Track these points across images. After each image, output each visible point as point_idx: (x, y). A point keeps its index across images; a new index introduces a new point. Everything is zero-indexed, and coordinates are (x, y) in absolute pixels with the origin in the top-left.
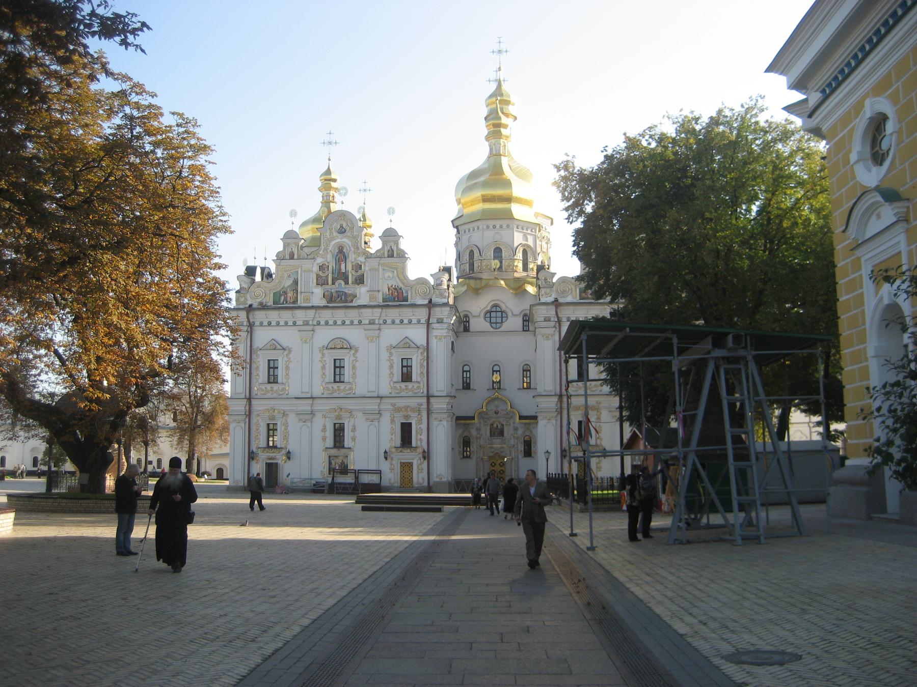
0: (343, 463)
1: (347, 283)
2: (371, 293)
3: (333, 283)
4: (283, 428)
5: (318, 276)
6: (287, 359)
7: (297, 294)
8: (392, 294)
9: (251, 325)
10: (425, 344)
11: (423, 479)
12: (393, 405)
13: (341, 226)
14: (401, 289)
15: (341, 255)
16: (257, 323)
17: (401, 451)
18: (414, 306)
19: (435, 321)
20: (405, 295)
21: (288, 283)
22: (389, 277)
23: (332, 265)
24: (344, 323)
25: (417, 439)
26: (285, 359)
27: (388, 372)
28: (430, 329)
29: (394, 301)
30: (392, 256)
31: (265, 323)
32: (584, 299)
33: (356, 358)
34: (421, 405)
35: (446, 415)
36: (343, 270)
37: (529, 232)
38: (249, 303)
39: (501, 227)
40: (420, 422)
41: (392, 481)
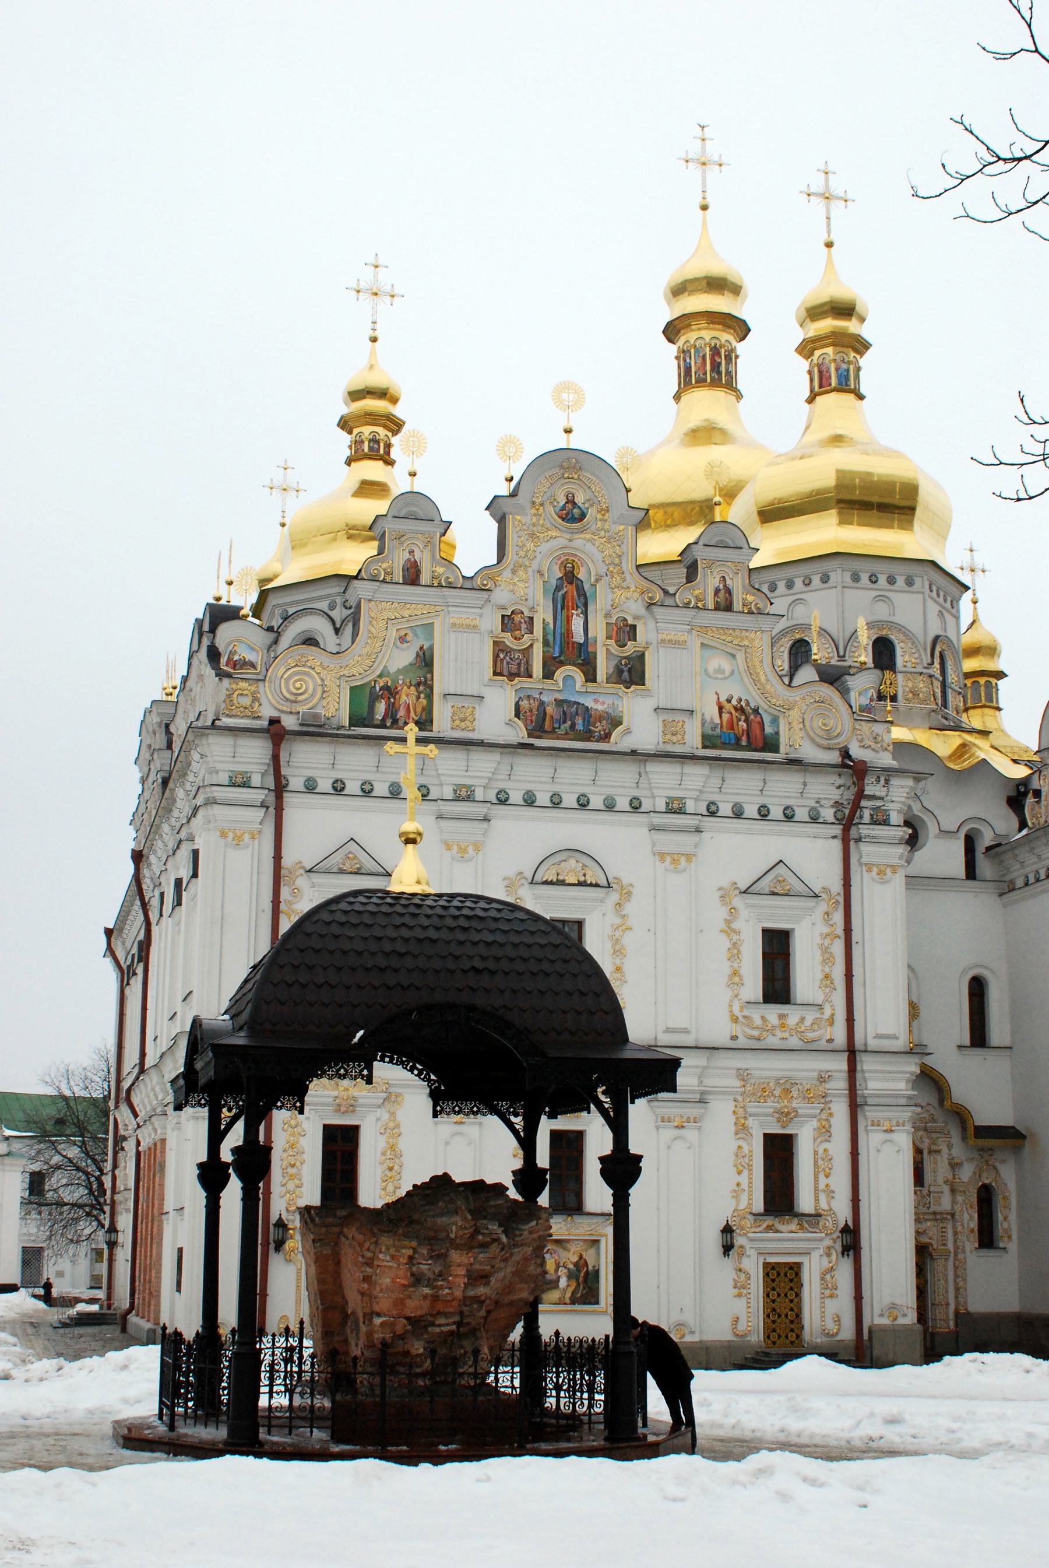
0: (581, 1263)
1: (591, 677)
2: (669, 717)
3: (548, 674)
4: (382, 1142)
7: (430, 697)
8: (731, 726)
9: (280, 789)
10: (837, 887)
11: (838, 1320)
12: (743, 1076)
13: (571, 501)
14: (756, 711)
16: (296, 782)
17: (770, 1228)
18: (794, 763)
19: (867, 818)
20: (769, 730)
21: (403, 658)
22: (719, 670)
23: (544, 615)
24: (583, 804)
25: (816, 1189)
27: (726, 969)
28: (852, 843)
29: (737, 746)
30: (728, 608)
31: (325, 785)
34: (822, 1079)
35: (907, 1114)
36: (579, 637)
37: (948, 605)
38: (267, 712)
39: (891, 580)
40: (825, 1132)
41: (742, 1327)
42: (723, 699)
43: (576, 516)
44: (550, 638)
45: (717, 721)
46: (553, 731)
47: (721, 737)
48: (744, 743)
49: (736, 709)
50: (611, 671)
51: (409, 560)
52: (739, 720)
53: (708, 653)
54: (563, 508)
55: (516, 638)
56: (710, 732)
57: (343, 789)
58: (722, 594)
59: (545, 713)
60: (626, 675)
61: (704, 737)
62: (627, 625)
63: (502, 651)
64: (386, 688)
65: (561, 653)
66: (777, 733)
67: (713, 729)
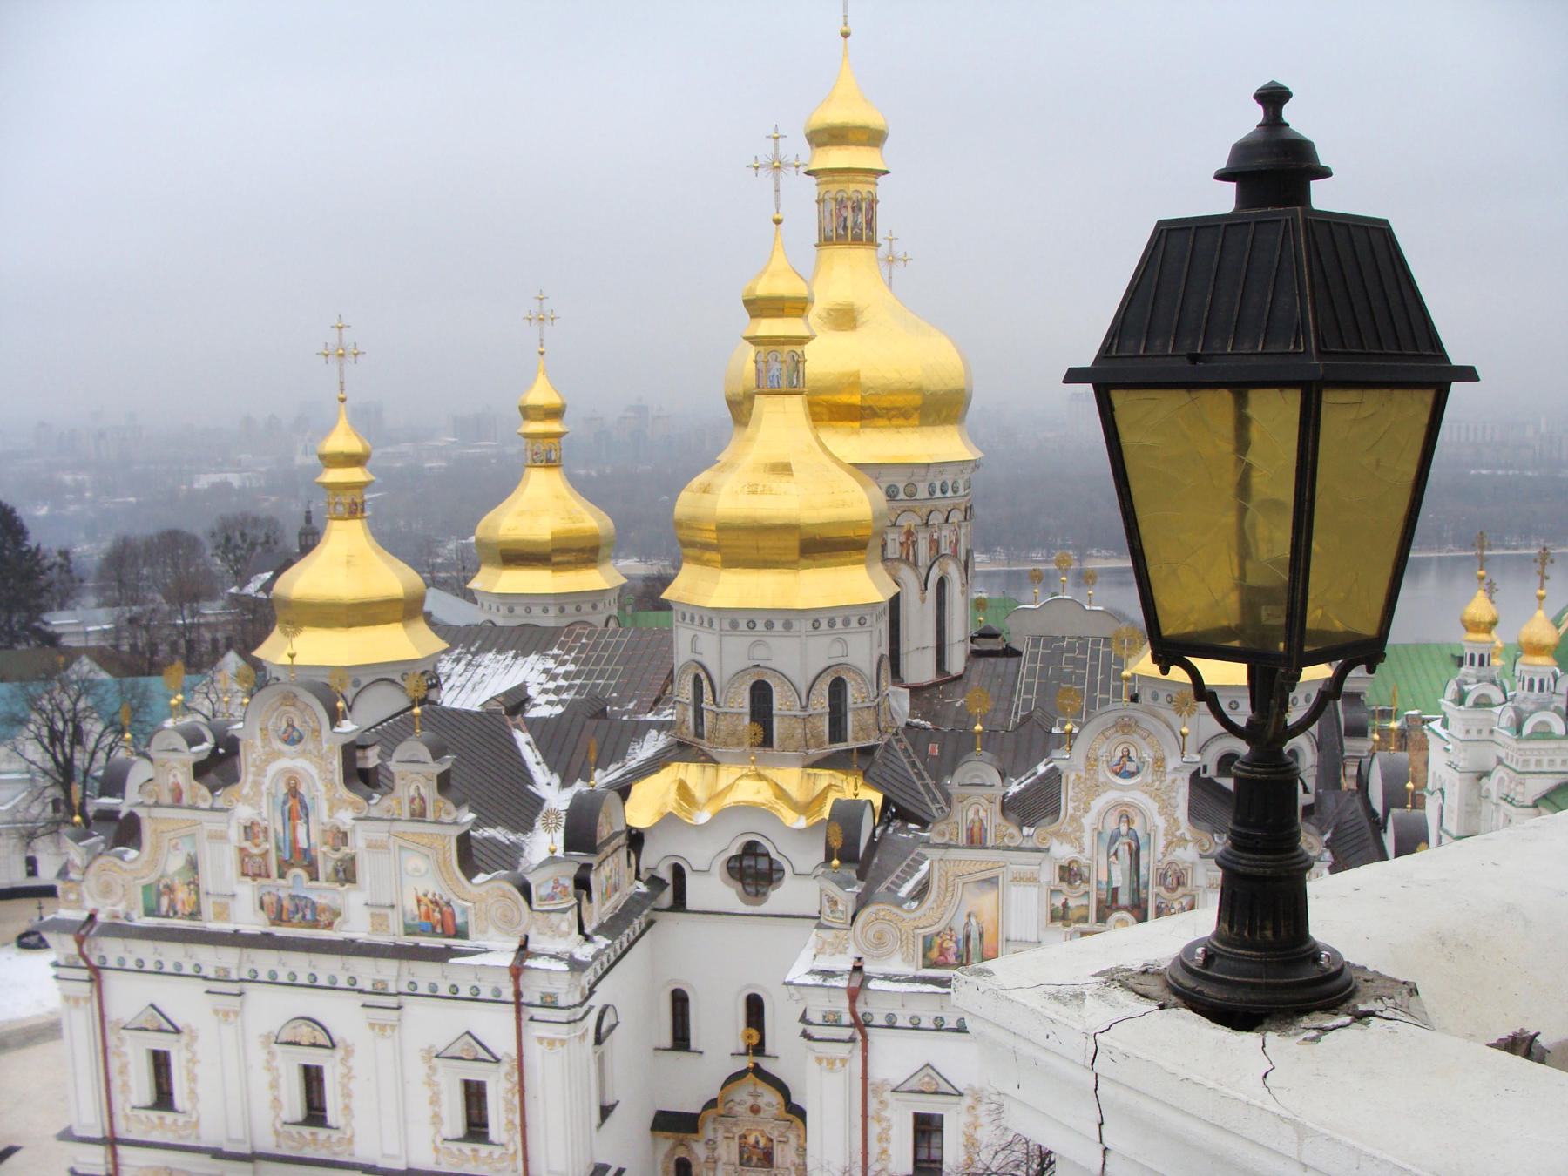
1: (314, 876)
2: (377, 911)
3: (282, 876)
5: (242, 850)
6: (189, 1055)
7: (197, 893)
8: (428, 916)
10: (514, 1053)
13: (291, 725)
14: (448, 904)
15: (295, 804)
16: (112, 962)
20: (459, 920)
22: (416, 870)
26: (185, 1055)
29: (433, 933)
32: (934, 965)
33: (350, 1069)
36: (303, 844)
42: (420, 894)
43: (296, 738)
44: (282, 845)
45: (417, 912)
46: (289, 921)
47: (416, 926)
48: (439, 930)
49: (432, 902)
50: (330, 869)
51: (173, 783)
52: (434, 911)
53: (404, 854)
54: (285, 733)
55: (257, 846)
56: (411, 922)
57: (141, 967)
58: (417, 802)
59: (282, 906)
60: (341, 874)
61: (406, 926)
62: (339, 831)
63: (246, 855)
64: (167, 886)
65: (291, 857)
66: (467, 923)
67: (413, 919)
